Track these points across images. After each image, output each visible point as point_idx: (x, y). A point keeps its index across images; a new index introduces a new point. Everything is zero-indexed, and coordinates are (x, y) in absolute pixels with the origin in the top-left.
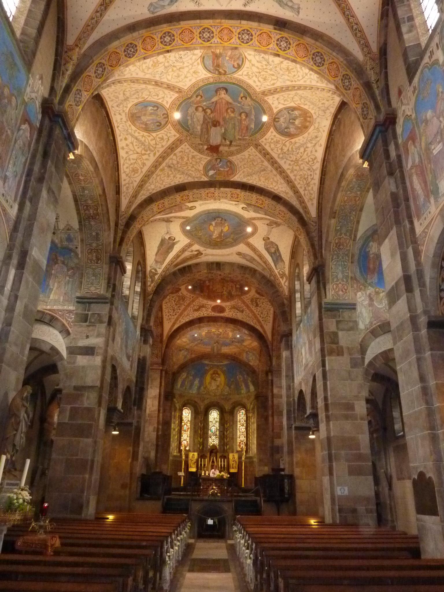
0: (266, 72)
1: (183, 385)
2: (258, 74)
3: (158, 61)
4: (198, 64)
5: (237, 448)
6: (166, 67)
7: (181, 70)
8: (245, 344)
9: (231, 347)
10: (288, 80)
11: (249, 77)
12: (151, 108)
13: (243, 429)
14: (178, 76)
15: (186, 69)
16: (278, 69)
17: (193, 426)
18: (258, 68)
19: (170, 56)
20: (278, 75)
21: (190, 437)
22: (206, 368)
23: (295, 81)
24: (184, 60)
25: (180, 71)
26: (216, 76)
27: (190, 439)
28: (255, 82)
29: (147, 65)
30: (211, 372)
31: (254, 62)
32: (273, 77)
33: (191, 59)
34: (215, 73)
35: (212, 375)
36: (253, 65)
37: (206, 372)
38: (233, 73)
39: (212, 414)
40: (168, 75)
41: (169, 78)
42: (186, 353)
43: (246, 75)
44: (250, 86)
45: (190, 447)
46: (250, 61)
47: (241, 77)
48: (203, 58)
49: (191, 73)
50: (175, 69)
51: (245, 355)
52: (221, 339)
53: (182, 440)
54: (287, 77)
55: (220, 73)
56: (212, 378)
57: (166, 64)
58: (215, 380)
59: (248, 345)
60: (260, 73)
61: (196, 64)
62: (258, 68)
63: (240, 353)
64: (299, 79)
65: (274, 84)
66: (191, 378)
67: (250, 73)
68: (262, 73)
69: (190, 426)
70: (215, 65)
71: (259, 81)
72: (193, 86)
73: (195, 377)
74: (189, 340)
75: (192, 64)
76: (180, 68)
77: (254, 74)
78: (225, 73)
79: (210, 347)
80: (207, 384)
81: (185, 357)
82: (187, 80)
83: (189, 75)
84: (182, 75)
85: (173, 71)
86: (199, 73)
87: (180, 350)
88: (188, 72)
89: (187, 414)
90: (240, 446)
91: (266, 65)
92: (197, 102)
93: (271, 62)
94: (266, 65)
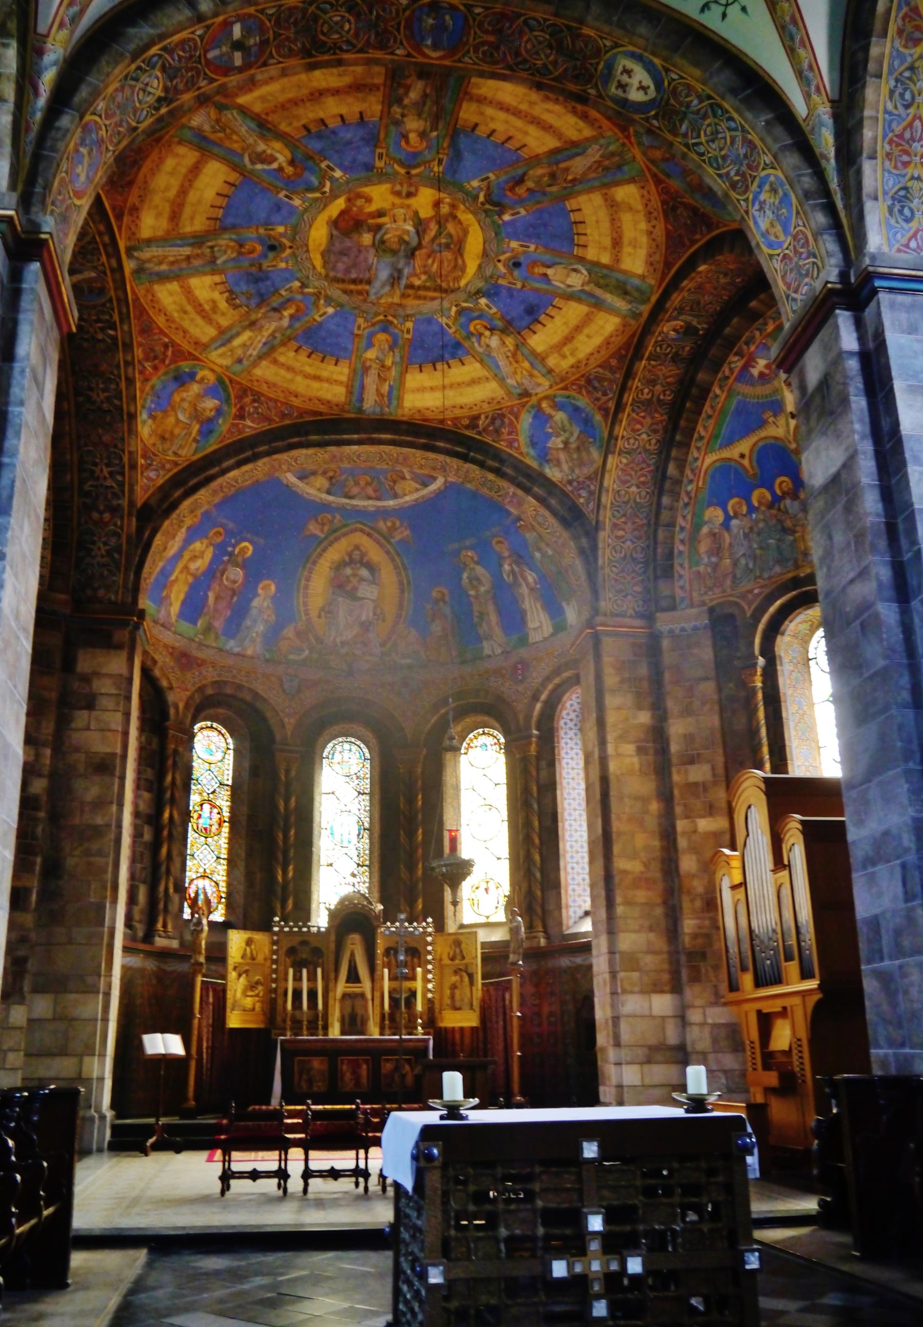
1: (193, 607)
8: (539, 341)
9: (459, 372)
17: (245, 809)
21: (231, 862)
22: (313, 528)
27: (229, 873)
30: (334, 554)
35: (339, 567)
37: (309, 552)
39: (338, 757)
42: (210, 404)
45: (229, 907)
51: (526, 421)
52: (412, 304)
53: (190, 875)
56: (340, 585)
58: (352, 595)
59: (558, 347)
63: (500, 417)
66: (236, 574)
69: (232, 810)
73: (256, 571)
74: (232, 297)
79: (342, 372)
80: (314, 613)
81: (207, 426)
87: (182, 380)
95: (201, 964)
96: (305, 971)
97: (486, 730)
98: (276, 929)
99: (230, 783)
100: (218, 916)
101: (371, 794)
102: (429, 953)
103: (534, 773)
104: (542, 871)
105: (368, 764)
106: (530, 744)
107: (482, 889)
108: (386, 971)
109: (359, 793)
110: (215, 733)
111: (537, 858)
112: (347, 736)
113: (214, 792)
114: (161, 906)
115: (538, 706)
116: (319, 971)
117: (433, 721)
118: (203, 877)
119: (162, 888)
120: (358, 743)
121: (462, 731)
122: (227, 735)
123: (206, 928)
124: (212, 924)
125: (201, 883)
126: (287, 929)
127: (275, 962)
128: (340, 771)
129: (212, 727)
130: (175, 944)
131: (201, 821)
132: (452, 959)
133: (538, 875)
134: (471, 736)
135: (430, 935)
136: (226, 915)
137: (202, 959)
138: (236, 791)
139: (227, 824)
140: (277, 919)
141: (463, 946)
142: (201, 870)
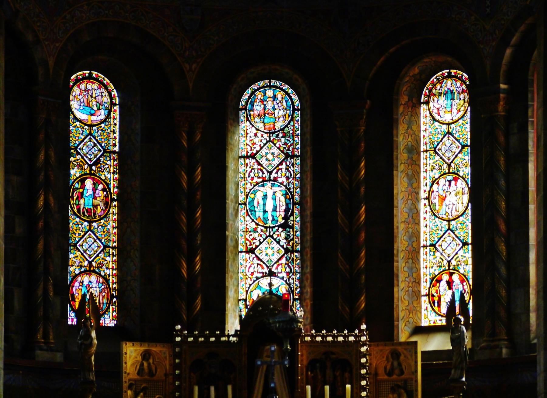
5: (415, 309)
13: (456, 198)
39: (258, 108)
53: (73, 269)
89: (92, 107)
90: (435, 302)
95: (92, 381)
96: (212, 389)
97: (453, 71)
98: (178, 339)
99: (117, 149)
100: (109, 321)
101: (302, 157)
102: (363, 366)
103: (502, 139)
104: (508, 264)
105: (297, 116)
106: (498, 101)
107: (443, 284)
108: (309, 388)
109: (287, 156)
110: (96, 86)
111: (502, 248)
112: (270, 79)
113: (97, 162)
114: (41, 313)
115: (508, 52)
116: (230, 388)
117: (379, 63)
118: (89, 271)
119: (40, 292)
120: (286, 87)
121: (420, 73)
122: (111, 86)
123: (95, 341)
124: (102, 331)
125: (86, 279)
126: (191, 339)
127: (178, 378)
128: (260, 126)
129: (90, 77)
130: (59, 357)
131: (82, 201)
132: (390, 373)
133: (503, 270)
134: (434, 78)
135: (364, 344)
136: (118, 318)
137: (92, 377)
138: (125, 160)
139: (115, 203)
140: (179, 327)
141: (402, 357)
142: (86, 263)
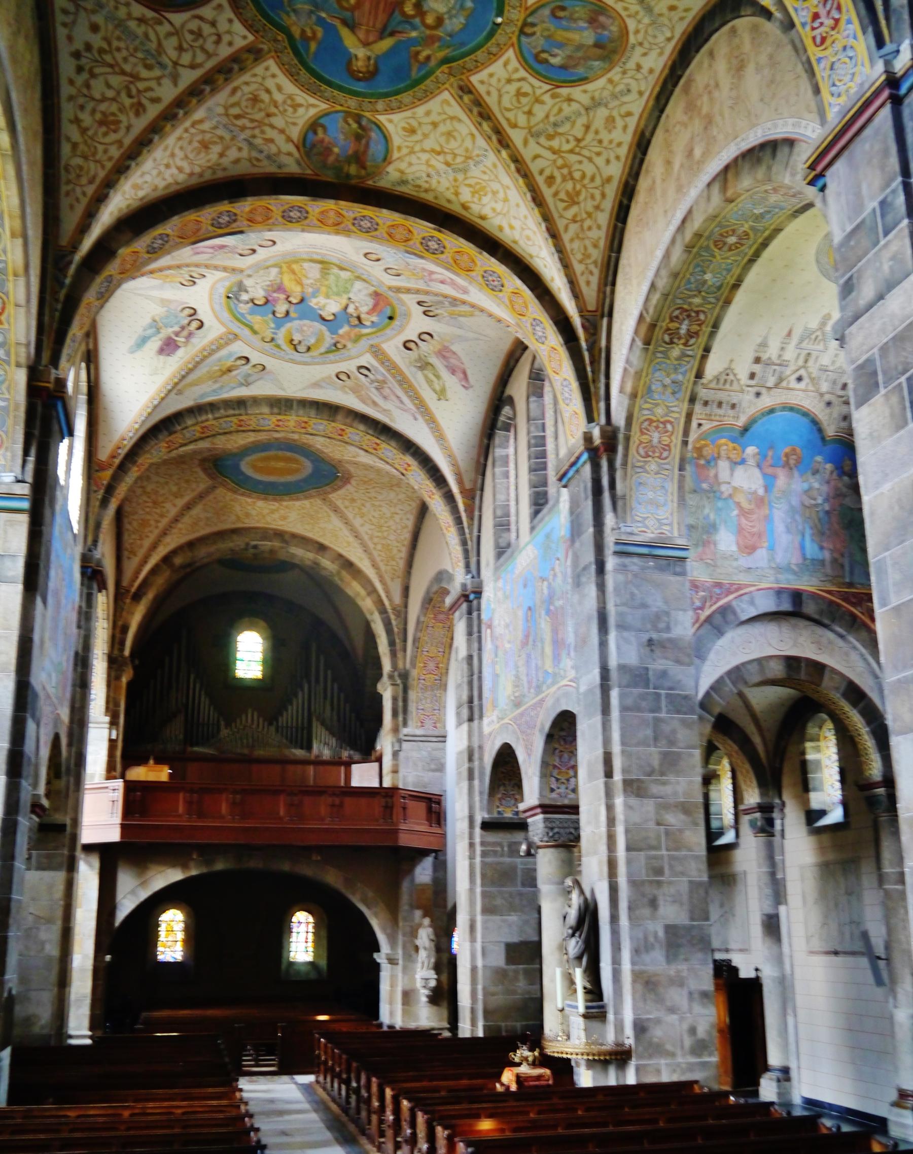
0: (252, 121)
2: (273, 110)
3: (473, 194)
4: (399, 148)
6: (465, 171)
7: (438, 148)
10: (201, 121)
11: (293, 100)
12: (553, 61)
14: (449, 135)
15: (429, 144)
16: (227, 136)
18: (272, 126)
19: (448, 189)
20: (224, 120)
23: (186, 130)
24: (424, 168)
25: (441, 146)
26: (367, 114)
28: (279, 88)
29: (493, 205)
31: (280, 140)
32: (235, 111)
33: (410, 164)
34: (369, 120)
36: (282, 131)
38: (327, 115)
40: (467, 150)
41: (468, 143)
43: (300, 105)
44: (292, 75)
46: (289, 140)
47: (312, 101)
48: (385, 159)
49: (419, 132)
50: (449, 158)
54: (206, 126)
55: (358, 118)
57: (460, 177)
60: (268, 115)
61: (405, 151)
62: (272, 126)
64: (180, 143)
65: (234, 91)
67: (290, 110)
68: (262, 114)
70: (364, 141)
71: (268, 91)
72: (428, 95)
75: (412, 152)
76: (439, 153)
77: (281, 109)
78: (348, 114)
82: (434, 117)
83: (427, 128)
84: (443, 134)
85: (455, 155)
86: (404, 129)
88: (426, 136)
91: (254, 137)
92: (433, 43)
93: (245, 146)
94: (254, 137)
